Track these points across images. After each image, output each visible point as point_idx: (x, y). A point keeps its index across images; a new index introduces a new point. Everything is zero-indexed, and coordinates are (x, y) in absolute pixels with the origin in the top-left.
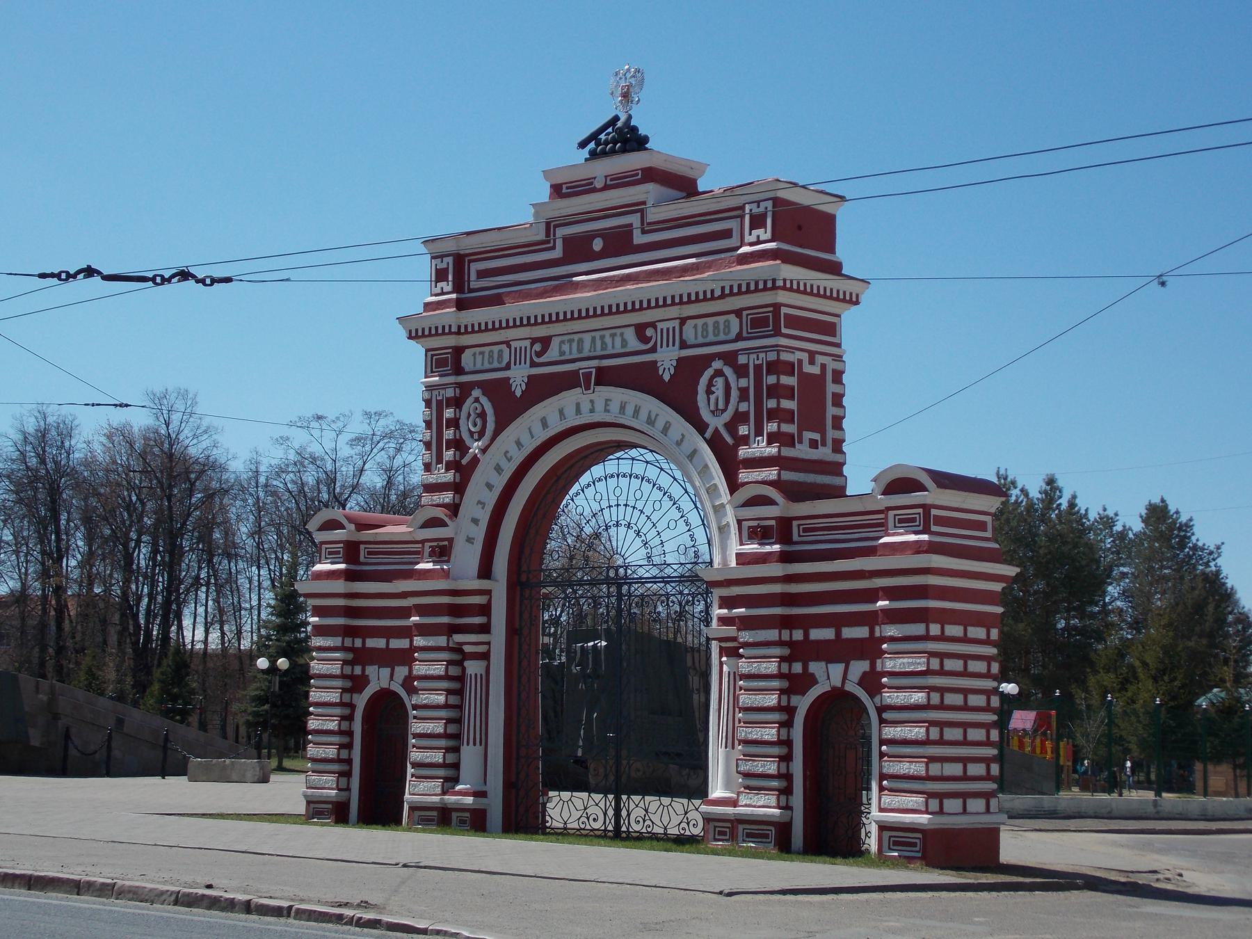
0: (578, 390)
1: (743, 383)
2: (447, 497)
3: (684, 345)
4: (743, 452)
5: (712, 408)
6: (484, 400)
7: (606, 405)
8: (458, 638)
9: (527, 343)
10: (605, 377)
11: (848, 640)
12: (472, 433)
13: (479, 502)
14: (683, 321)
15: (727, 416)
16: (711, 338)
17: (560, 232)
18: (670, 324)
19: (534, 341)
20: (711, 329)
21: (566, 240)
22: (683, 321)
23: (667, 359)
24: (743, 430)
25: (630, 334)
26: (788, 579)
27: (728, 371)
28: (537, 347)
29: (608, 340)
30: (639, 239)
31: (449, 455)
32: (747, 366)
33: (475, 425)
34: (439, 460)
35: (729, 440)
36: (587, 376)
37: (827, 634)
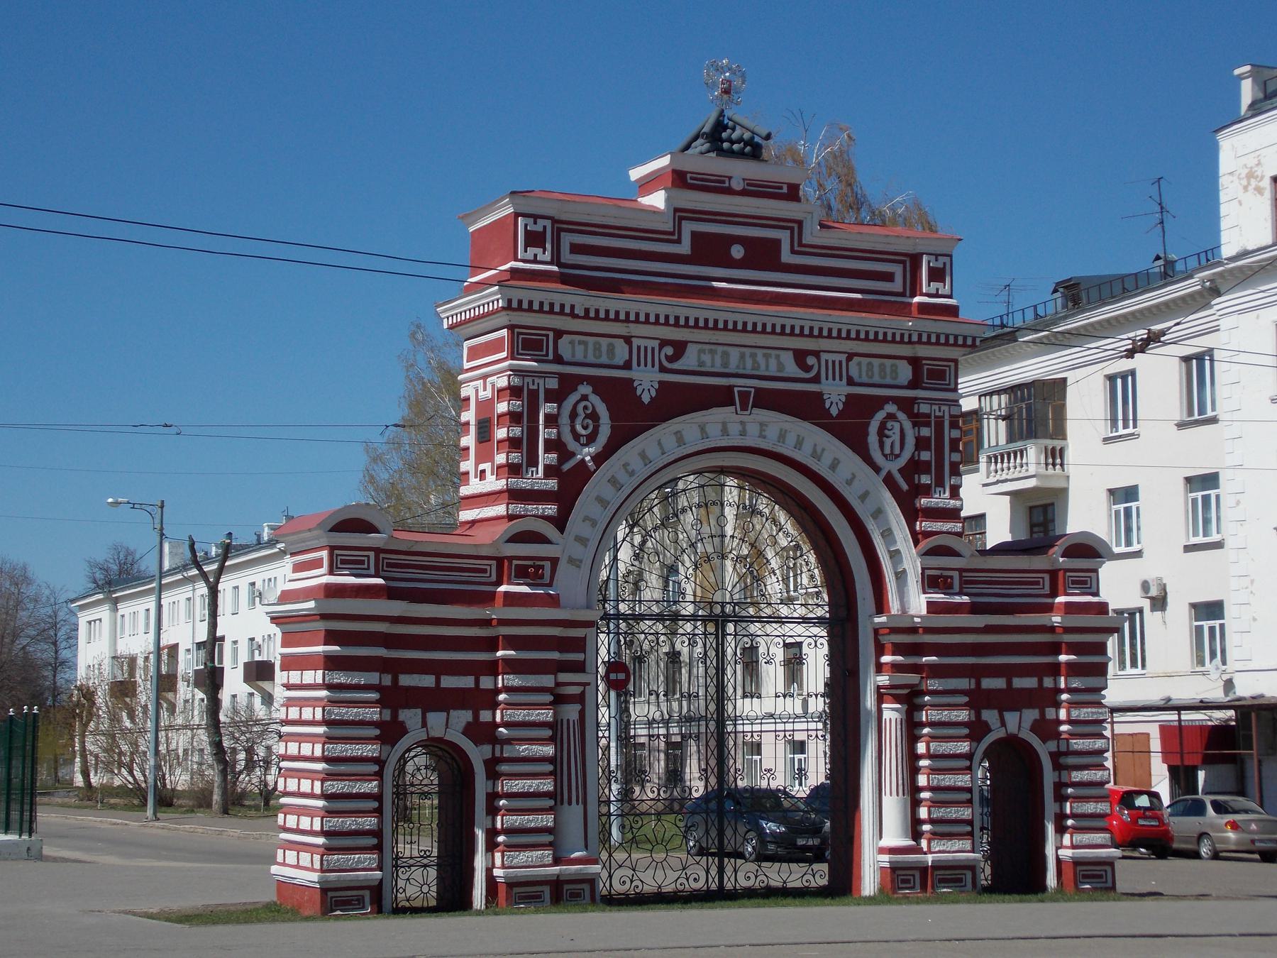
0: (732, 409)
1: (925, 432)
2: (551, 509)
3: (851, 382)
4: (924, 501)
5: (887, 451)
6: (595, 399)
7: (762, 430)
8: (563, 677)
9: (656, 344)
10: (766, 400)
11: (1018, 690)
12: (577, 437)
13: (586, 519)
14: (850, 356)
15: (902, 462)
16: (876, 379)
17: (688, 228)
18: (837, 357)
19: (664, 343)
20: (876, 370)
21: (695, 235)
22: (850, 356)
23: (835, 394)
24: (925, 479)
25: (788, 360)
26: (988, 629)
27: (901, 416)
28: (669, 351)
29: (760, 359)
30: (786, 257)
31: (553, 457)
32: (928, 416)
33: (585, 428)
34: (533, 461)
35: (905, 487)
36: (744, 396)
37: (998, 683)
